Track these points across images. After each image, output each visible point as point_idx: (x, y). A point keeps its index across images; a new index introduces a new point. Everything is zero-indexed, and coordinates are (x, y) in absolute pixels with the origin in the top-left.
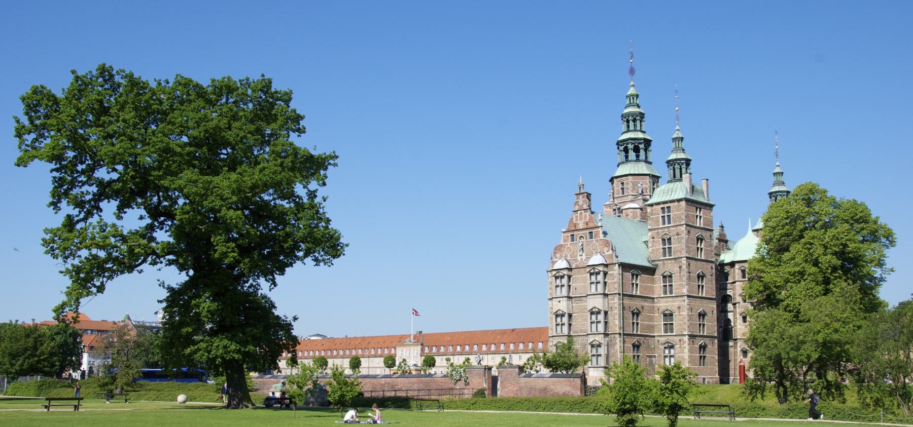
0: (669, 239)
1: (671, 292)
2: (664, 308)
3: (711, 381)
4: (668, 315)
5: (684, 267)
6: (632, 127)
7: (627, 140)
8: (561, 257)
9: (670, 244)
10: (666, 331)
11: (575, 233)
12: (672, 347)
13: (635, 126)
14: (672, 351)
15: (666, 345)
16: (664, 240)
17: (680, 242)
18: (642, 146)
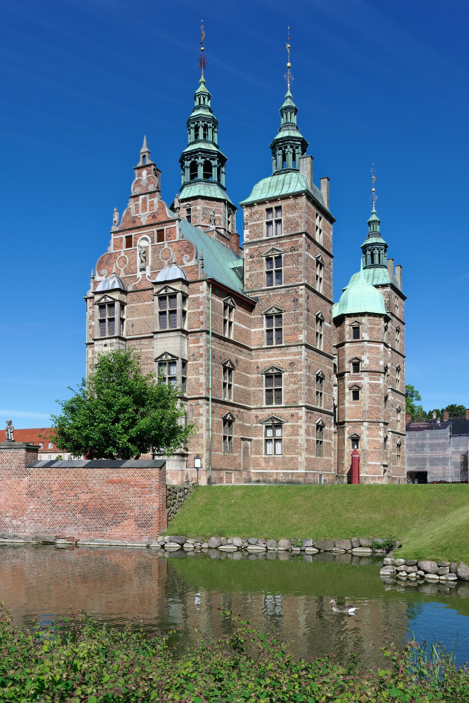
0: (279, 258)
1: (279, 340)
2: (268, 365)
3: (327, 478)
4: (273, 376)
5: (302, 300)
6: (201, 137)
7: (197, 151)
8: (109, 273)
9: (279, 264)
10: (269, 401)
11: (133, 234)
12: (279, 426)
13: (205, 136)
14: (278, 432)
15: (270, 423)
16: (269, 260)
17: (296, 262)
18: (214, 163)
